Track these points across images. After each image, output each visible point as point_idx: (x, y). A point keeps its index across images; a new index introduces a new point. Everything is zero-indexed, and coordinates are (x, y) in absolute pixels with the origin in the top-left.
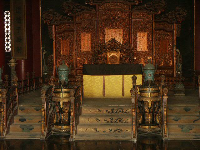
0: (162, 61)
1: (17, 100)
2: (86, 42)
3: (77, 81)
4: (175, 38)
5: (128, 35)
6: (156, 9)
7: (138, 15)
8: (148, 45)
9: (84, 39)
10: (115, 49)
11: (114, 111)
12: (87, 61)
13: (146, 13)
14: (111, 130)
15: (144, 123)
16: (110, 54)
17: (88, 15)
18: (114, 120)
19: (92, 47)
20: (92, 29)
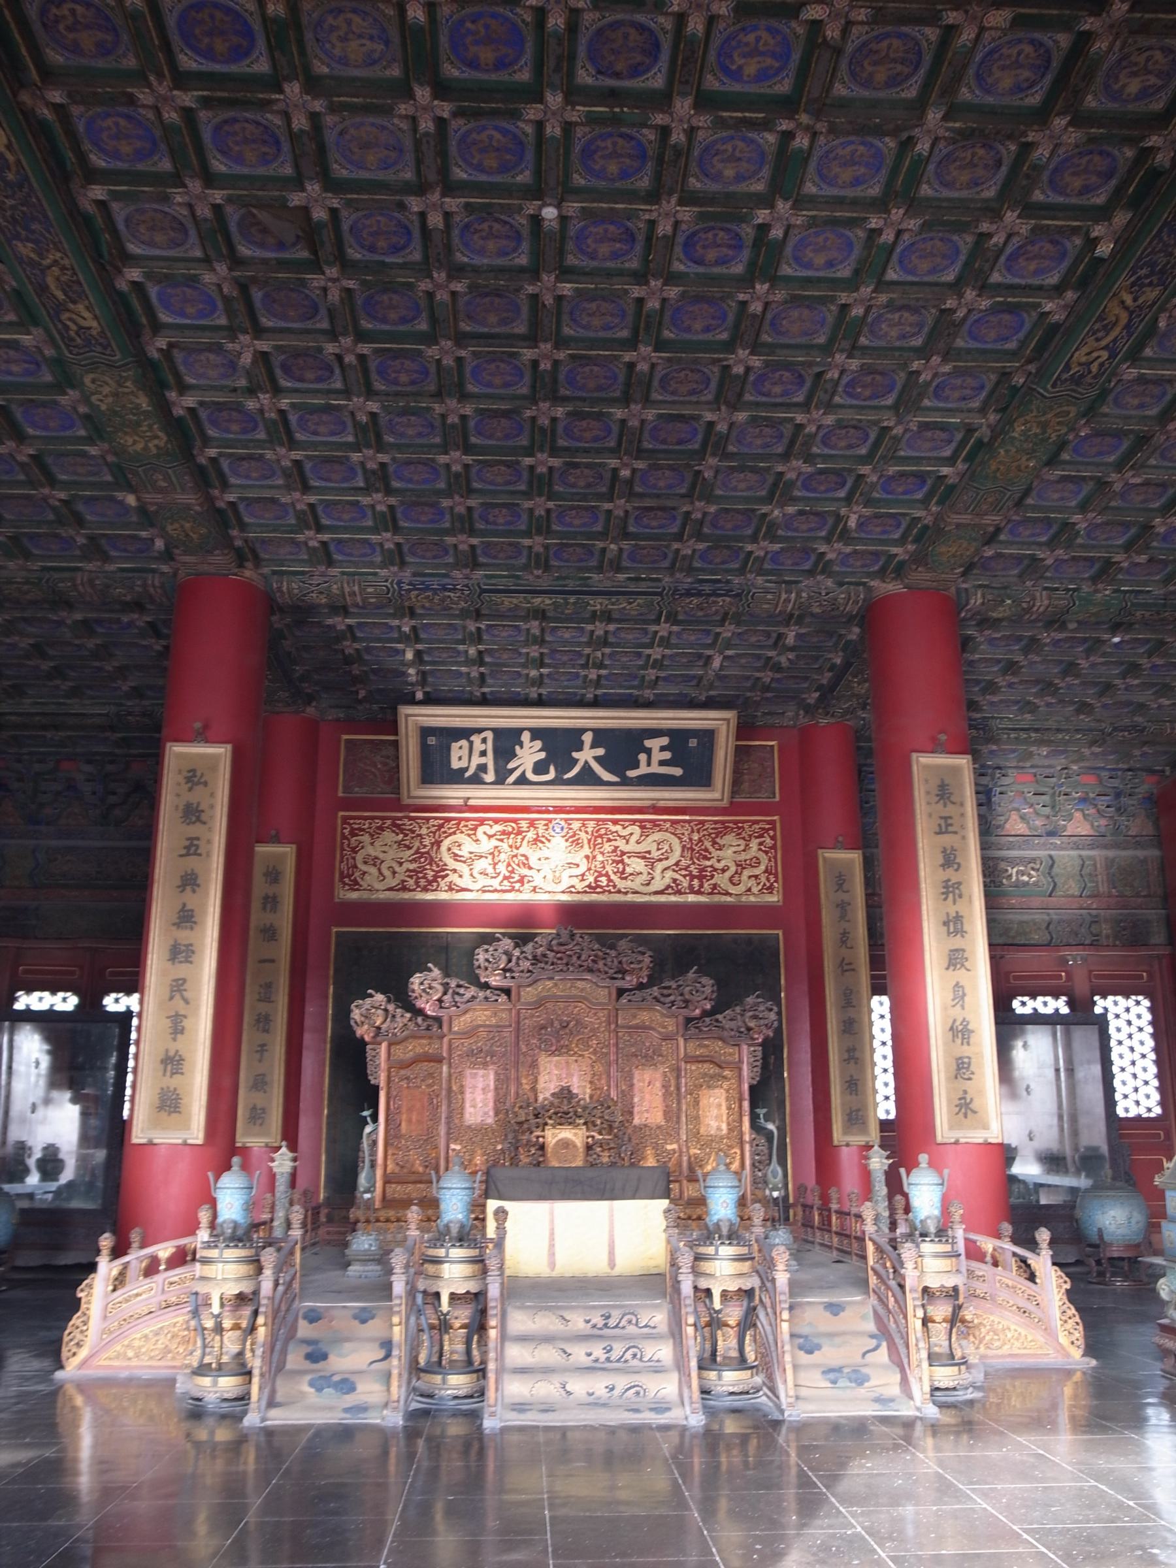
0: (709, 1154)
1: (296, 1285)
4: (746, 1087)
6: (687, 1002)
7: (635, 1017)
9: (475, 1087)
11: (612, 1322)
14: (612, 1389)
15: (709, 1361)
16: (554, 1135)
18: (614, 1355)
19: (496, 1114)
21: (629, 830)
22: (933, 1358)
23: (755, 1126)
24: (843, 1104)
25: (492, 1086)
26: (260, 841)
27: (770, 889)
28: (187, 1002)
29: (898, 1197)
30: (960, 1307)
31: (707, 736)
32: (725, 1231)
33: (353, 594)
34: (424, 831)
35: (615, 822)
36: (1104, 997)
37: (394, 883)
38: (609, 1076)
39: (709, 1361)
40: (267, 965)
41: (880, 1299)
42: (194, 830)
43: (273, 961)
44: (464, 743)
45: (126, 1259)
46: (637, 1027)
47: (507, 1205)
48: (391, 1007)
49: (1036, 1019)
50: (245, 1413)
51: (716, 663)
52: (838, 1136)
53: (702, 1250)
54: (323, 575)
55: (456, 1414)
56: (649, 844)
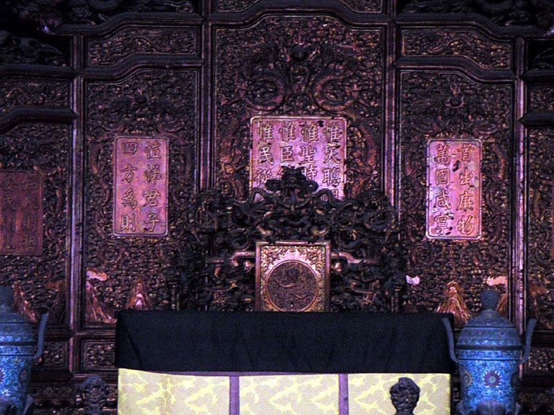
2: (140, 189)
3: (81, 405)
5: (373, 151)
7: (432, 40)
8: (489, 208)
9: (131, 169)
10: (303, 225)
12: (146, 291)
13: (478, 29)
16: (272, 257)
17: (153, 33)
19: (172, 217)
20: (175, 113)
25: (164, 169)
38: (381, 154)
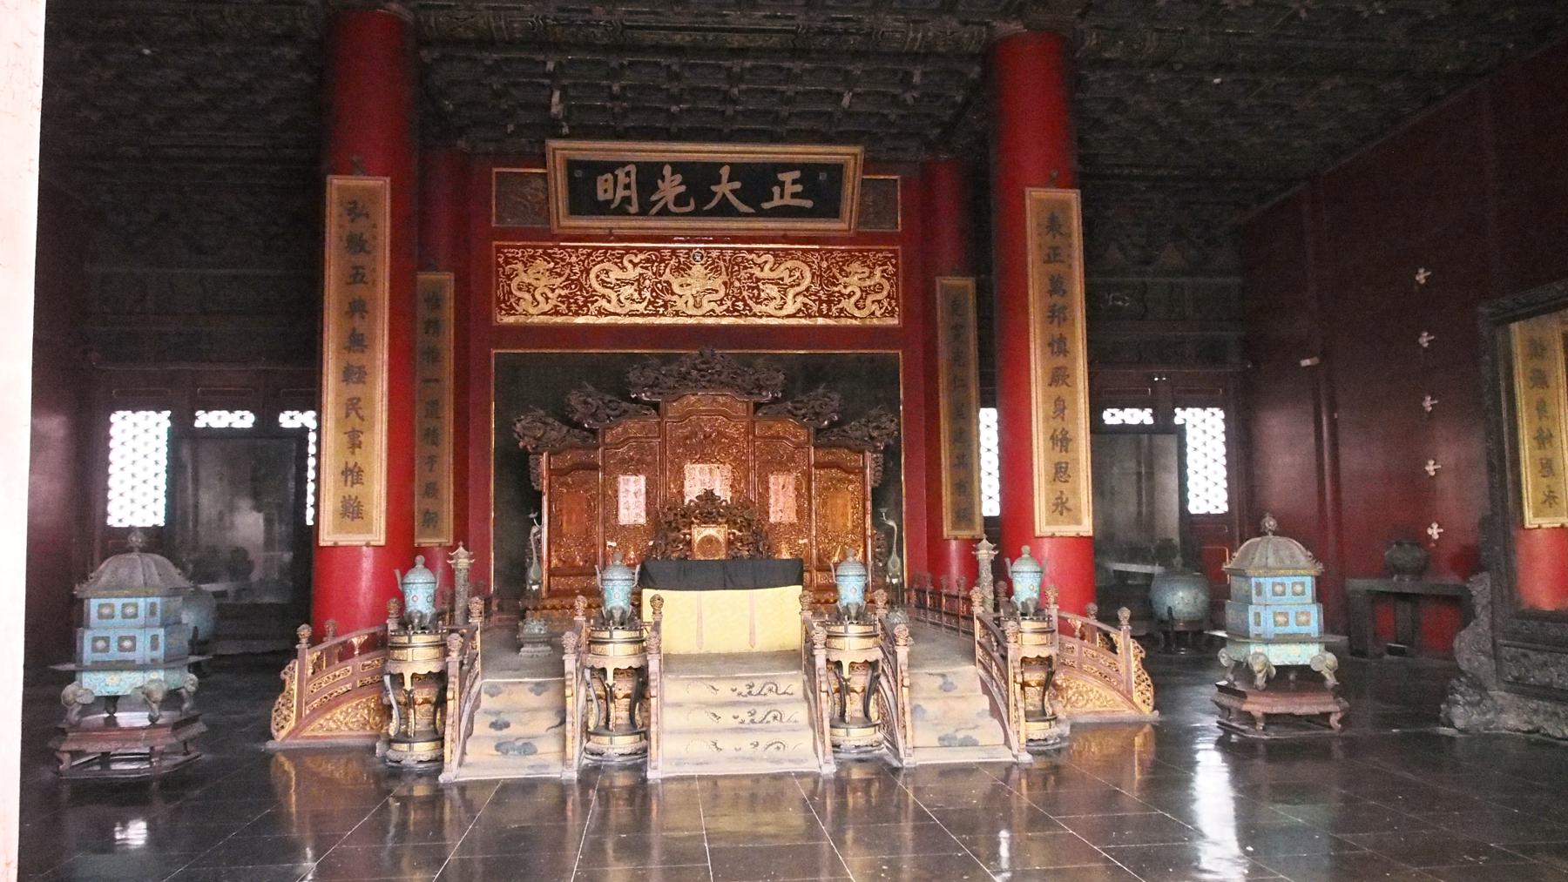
0: (835, 548)
1: (478, 665)
2: (631, 500)
6: (817, 414)
7: (770, 428)
11: (754, 691)
15: (841, 719)
18: (758, 718)
19: (648, 514)
21: (764, 258)
22: (1029, 716)
23: (877, 523)
24: (953, 503)
26: (422, 269)
27: (892, 313)
28: (362, 419)
29: (1002, 583)
30: (1053, 673)
31: (836, 170)
32: (853, 613)
33: (499, 28)
34: (574, 259)
35: (750, 251)
36: (1184, 408)
37: (547, 308)
38: (748, 483)
39: (841, 719)
40: (432, 384)
41: (985, 668)
42: (361, 259)
43: (437, 380)
44: (609, 176)
45: (323, 646)
46: (772, 437)
47: (663, 593)
48: (550, 420)
49: (1123, 429)
50: (440, 771)
51: (846, 101)
52: (947, 531)
53: (833, 629)
54: (470, 8)
55: (623, 768)
56: (782, 272)
